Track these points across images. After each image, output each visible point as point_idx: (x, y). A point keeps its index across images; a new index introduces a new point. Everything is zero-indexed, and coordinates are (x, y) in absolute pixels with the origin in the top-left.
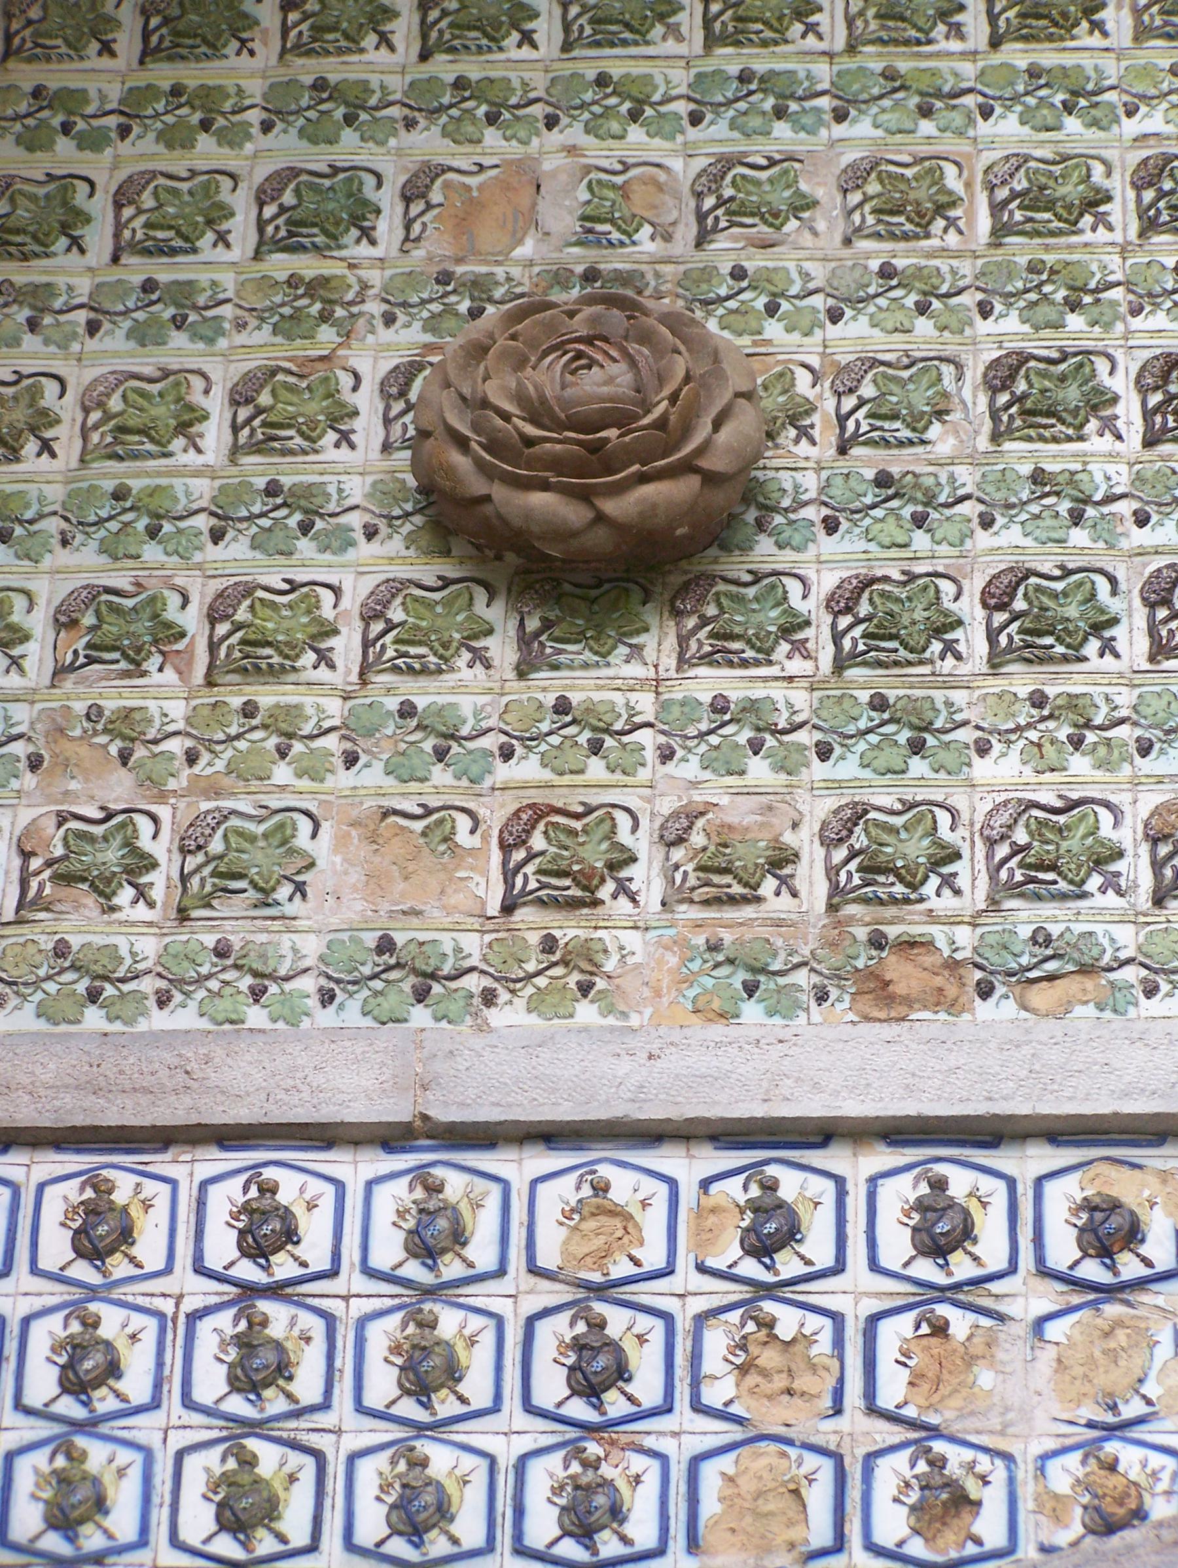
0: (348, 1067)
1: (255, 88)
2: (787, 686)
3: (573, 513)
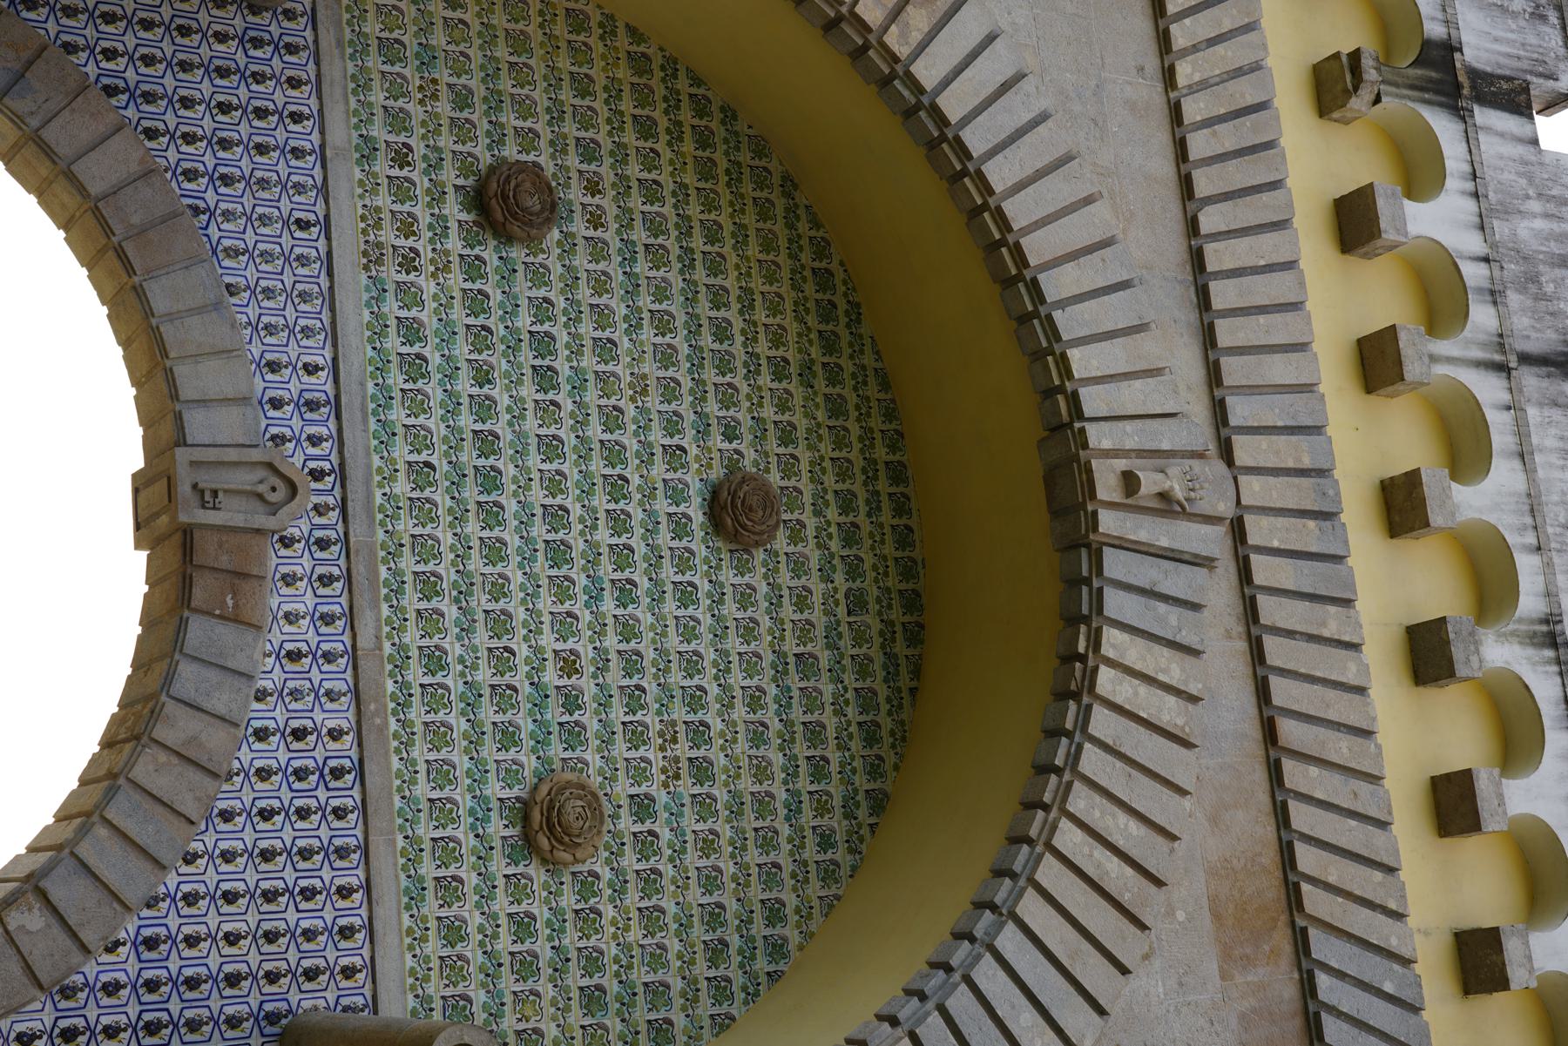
0: (341, 133)
1: (625, 140)
2: (454, 243)
3: (491, 194)
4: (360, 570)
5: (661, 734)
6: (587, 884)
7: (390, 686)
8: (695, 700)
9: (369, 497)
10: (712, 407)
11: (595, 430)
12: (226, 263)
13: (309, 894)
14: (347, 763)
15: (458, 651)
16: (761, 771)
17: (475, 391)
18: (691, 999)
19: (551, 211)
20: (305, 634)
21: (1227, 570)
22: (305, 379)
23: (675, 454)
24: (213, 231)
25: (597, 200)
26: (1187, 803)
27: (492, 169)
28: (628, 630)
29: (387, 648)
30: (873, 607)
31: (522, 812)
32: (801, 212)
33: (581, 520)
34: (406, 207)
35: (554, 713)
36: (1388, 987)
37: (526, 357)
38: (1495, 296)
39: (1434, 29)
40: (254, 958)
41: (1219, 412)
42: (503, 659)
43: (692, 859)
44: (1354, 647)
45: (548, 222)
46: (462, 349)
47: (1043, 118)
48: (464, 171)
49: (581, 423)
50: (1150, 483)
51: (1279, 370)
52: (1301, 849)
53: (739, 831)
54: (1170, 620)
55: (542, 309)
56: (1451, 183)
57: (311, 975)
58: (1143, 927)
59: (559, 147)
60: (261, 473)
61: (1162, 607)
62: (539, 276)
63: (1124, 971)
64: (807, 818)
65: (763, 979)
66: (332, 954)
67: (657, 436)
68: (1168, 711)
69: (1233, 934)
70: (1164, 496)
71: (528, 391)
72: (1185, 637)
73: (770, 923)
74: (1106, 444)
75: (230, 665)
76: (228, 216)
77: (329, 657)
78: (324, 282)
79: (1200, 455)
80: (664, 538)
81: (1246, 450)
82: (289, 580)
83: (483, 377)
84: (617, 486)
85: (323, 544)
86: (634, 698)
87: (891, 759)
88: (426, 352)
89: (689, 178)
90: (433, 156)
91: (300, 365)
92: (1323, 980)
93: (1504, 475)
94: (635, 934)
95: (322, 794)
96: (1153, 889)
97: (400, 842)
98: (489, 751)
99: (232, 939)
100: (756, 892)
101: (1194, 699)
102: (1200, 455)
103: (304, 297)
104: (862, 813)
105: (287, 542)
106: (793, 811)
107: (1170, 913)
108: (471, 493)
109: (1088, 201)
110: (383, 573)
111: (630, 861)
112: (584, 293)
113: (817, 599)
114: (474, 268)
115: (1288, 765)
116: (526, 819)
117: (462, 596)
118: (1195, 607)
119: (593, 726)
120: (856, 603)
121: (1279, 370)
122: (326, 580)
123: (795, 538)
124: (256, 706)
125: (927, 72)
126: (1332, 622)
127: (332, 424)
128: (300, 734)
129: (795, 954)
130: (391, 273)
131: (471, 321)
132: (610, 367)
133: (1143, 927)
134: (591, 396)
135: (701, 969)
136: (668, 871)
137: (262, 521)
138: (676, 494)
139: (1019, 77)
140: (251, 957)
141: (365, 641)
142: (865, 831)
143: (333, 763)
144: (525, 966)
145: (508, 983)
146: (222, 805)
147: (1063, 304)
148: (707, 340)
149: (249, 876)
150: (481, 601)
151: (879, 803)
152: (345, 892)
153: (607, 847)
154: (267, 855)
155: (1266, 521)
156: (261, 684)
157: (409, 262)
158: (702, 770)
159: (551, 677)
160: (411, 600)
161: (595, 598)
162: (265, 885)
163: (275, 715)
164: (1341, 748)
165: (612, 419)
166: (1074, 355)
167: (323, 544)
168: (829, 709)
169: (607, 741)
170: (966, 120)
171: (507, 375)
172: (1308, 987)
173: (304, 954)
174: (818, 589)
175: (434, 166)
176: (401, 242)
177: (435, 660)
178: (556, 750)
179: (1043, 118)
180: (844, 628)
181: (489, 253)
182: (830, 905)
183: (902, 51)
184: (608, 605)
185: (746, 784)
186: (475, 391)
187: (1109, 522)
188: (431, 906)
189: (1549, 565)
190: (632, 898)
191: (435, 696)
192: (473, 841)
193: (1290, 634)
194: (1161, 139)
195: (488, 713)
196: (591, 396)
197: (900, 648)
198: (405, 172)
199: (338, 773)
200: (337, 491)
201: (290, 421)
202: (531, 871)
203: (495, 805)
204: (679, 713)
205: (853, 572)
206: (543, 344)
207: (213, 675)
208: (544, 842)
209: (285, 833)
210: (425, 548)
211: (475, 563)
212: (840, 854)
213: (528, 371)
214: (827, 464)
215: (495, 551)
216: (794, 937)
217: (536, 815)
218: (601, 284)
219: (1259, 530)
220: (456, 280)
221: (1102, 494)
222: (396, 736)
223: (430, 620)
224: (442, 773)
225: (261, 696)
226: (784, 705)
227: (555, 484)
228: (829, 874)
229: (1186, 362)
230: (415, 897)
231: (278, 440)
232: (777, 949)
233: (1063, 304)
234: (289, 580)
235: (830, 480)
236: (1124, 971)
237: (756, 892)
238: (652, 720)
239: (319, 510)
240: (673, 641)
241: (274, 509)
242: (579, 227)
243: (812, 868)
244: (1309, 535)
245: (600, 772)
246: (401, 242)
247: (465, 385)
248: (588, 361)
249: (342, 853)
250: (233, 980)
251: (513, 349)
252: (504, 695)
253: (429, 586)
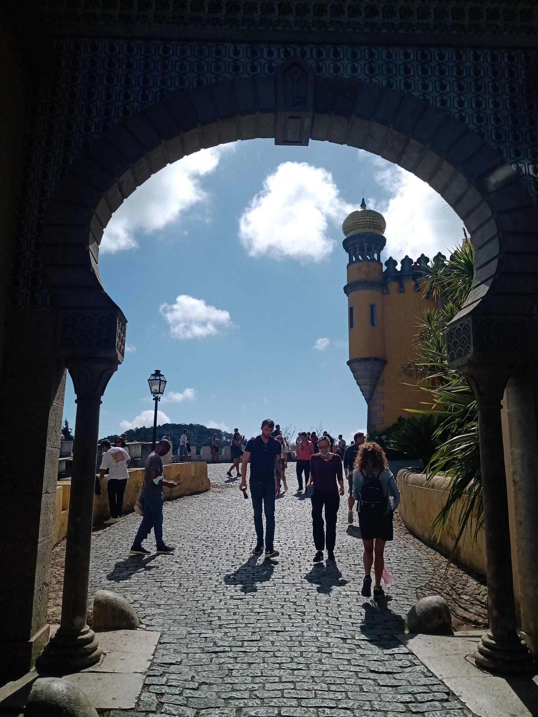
12: (187, 85)
14: (419, 52)
22: (241, 56)
29: (367, 30)
77: (372, 55)
82: (337, 69)
91: (235, 57)
95: (433, 64)
110: (332, 29)
124: (394, 88)
127: (263, 46)
143: (419, 58)
146: (439, 105)
156: (384, 84)
167: (319, 54)
225: (390, 85)
234: (337, 69)
239: (303, 54)
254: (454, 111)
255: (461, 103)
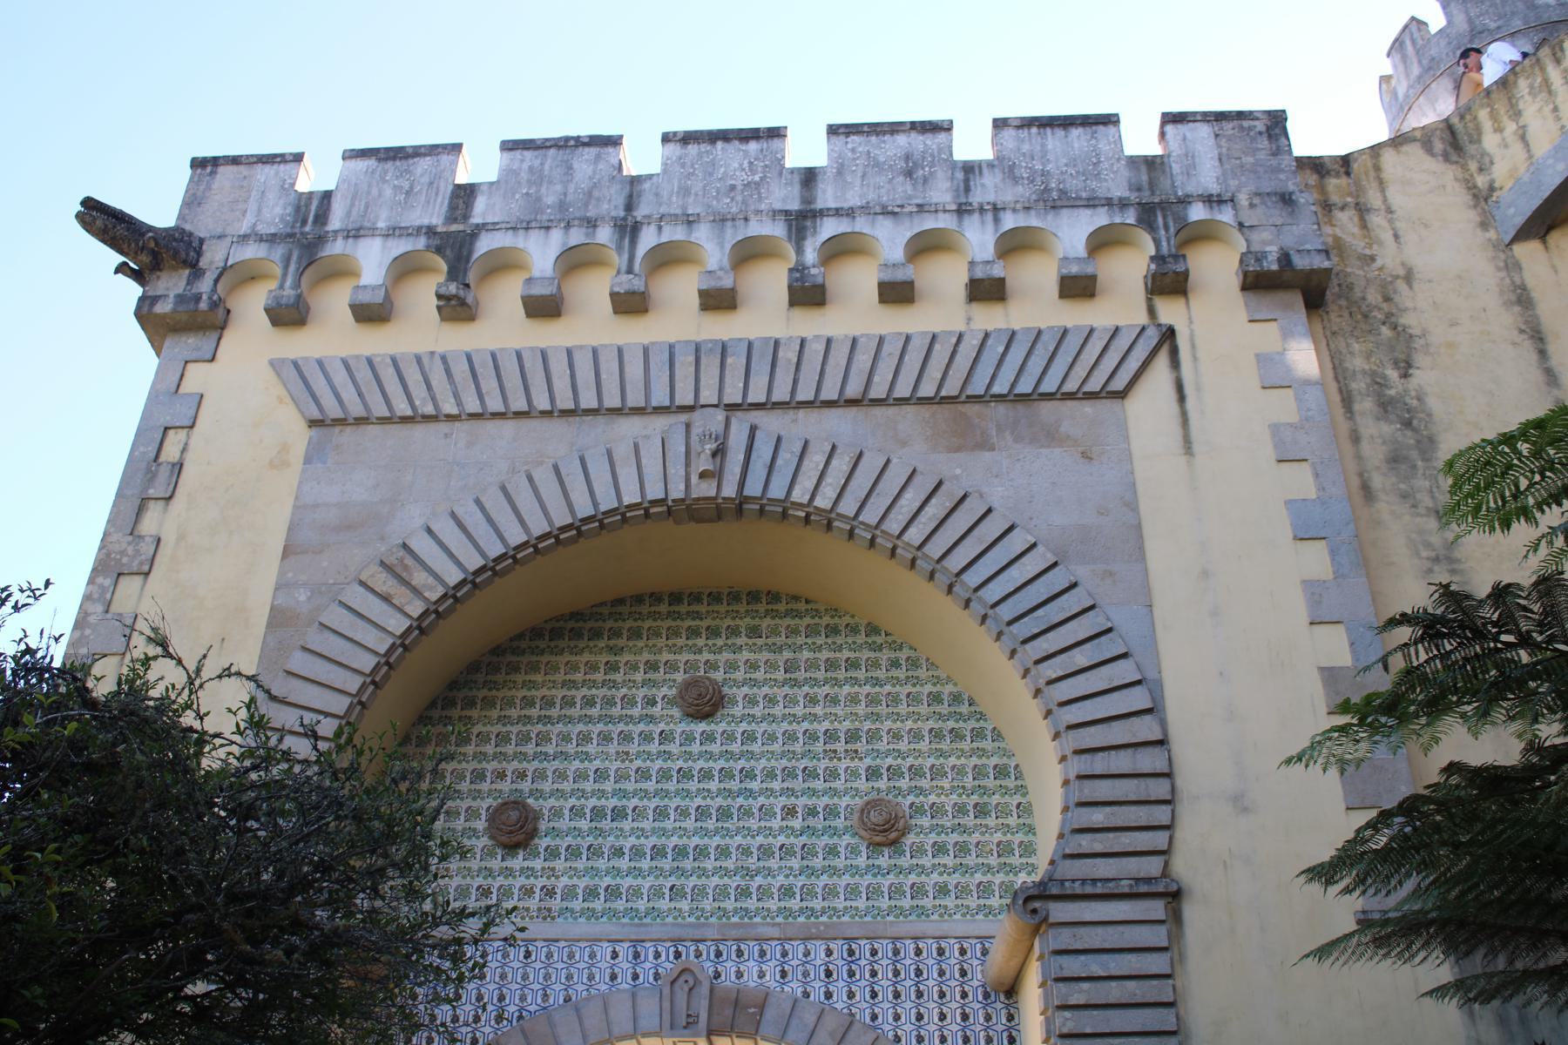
2: (538, 864)
4: (734, 933)
5: (831, 759)
6: (917, 810)
7: (802, 919)
8: (812, 737)
9: (690, 925)
10: (636, 712)
11: (650, 786)
13: (919, 972)
15: (781, 878)
16: (854, 699)
17: (627, 857)
18: (982, 753)
19: (518, 804)
20: (771, 967)
21: (757, 417)
23: (665, 737)
24: (533, 1008)
25: (509, 773)
26: (895, 461)
27: (492, 837)
28: (771, 775)
29: (779, 920)
30: (757, 622)
31: (875, 847)
32: (515, 644)
33: (704, 798)
34: (516, 891)
35: (818, 823)
36: (1001, 349)
37: (606, 824)
38: (592, 224)
39: (421, 242)
40: (954, 1005)
41: (660, 410)
42: (786, 851)
43: (903, 746)
44: (803, 342)
45: (525, 806)
46: (601, 864)
47: (478, 502)
48: (492, 855)
49: (646, 794)
50: (704, 463)
51: (635, 370)
52: (922, 393)
53: (888, 717)
54: (787, 459)
55: (576, 813)
56: (521, 245)
57: (963, 973)
58: (964, 497)
59: (477, 795)
60: (677, 985)
61: (779, 462)
62: (557, 813)
63: (989, 511)
64: (881, 674)
65: (973, 709)
66: (953, 957)
67: (654, 747)
68: (841, 465)
69: (970, 440)
70: (714, 455)
71: (627, 825)
72: (798, 448)
73: (940, 702)
74: (682, 487)
75: (788, 1011)
76: (523, 998)
77: (784, 954)
78: (562, 944)
79: (688, 426)
80: (715, 748)
81: (685, 397)
82: (739, 975)
83: (618, 852)
84: (685, 775)
85: (719, 954)
86: (810, 774)
87: (847, 619)
88: (604, 885)
89: (495, 714)
90: (484, 873)
92: (996, 389)
93: (703, 235)
94: (946, 783)
95: (863, 962)
96: (944, 487)
97: (891, 918)
98: (840, 863)
99: (942, 1017)
100: (923, 709)
101: (834, 447)
102: (688, 426)
103: (571, 956)
104: (879, 640)
105: (717, 975)
106: (877, 682)
107: (957, 477)
108: (688, 864)
109: (530, 479)
110: (735, 919)
111: (904, 784)
112: (567, 786)
113: (752, 656)
114: (552, 853)
115: (873, 395)
116: (879, 844)
117: (750, 874)
118: (779, 439)
119: (826, 800)
120: (754, 632)
121: (635, 370)
122: (740, 953)
123: (715, 667)
125: (454, 576)
126: (788, 355)
127: (648, 945)
128: (829, 974)
129: (958, 689)
130: (556, 903)
131: (584, 857)
132: (612, 774)
133: (964, 497)
134: (630, 786)
135: (966, 745)
136: (910, 761)
137: (704, 990)
138: (689, 738)
139: (453, 515)
140: (953, 1006)
141: (775, 932)
142: (889, 639)
144: (962, 849)
145: (971, 860)
146: (868, 1020)
147: (595, 504)
148: (595, 712)
149: (908, 1006)
150: (752, 862)
151: (873, 629)
152: (918, 952)
153: (896, 796)
154: (897, 995)
155: (728, 390)
156: (799, 994)
157: (550, 892)
158: (852, 736)
159: (797, 823)
160: (752, 903)
161: (750, 793)
162: (913, 997)
163: (817, 988)
164: (863, 360)
165: (643, 774)
166: (627, 500)
167: (719, 954)
168: (817, 655)
169: (834, 793)
170: (482, 554)
171: (617, 837)
172: (1000, 398)
173: (952, 977)
174: (746, 655)
175: (490, 873)
176: (537, 896)
177: (787, 892)
178: (839, 823)
179: (478, 502)
180: (770, 641)
181: (543, 843)
182: (932, 665)
183: (440, 591)
184: (755, 785)
185: (861, 709)
186: (627, 857)
187: (729, 491)
188: (927, 902)
189: (758, 212)
190: (925, 783)
191: (807, 892)
192: (891, 876)
193: (795, 382)
194: (491, 426)
195: (818, 862)
196: (630, 786)
197: (782, 607)
198: (494, 891)
199: (851, 952)
200: (688, 944)
201: (647, 968)
202: (908, 843)
203: (870, 862)
204: (819, 747)
205: (734, 632)
206: (598, 813)
207: (794, 1022)
208: (893, 835)
209: (884, 984)
210: (722, 893)
211: (730, 864)
212: (903, 655)
213: (615, 824)
214: (670, 642)
215: (723, 852)
216: (949, 688)
217: (878, 839)
218: (561, 775)
219: (733, 395)
220: (559, 864)
221: (713, 493)
222: (830, 917)
223: (764, 893)
224: (852, 892)
225: (806, 995)
226: (815, 682)
227: (683, 813)
228: (914, 663)
229: (630, 427)
230: (922, 912)
231: (657, 976)
232: (956, 699)
233: (595, 504)
234: (739, 975)
235: (681, 642)
236: (989, 511)
237: (923, 709)
238: (824, 764)
239: (698, 955)
240: (777, 747)
241: (697, 982)
242: (526, 786)
243: (910, 673)
244: (736, 362)
245: (853, 797)
246: (537, 896)
247: (624, 863)
248: (608, 786)
249: (896, 952)
250: (965, 1017)
251: (601, 833)
252: (808, 852)
253: (744, 893)
254: (886, 1027)
255: (897, 1017)
